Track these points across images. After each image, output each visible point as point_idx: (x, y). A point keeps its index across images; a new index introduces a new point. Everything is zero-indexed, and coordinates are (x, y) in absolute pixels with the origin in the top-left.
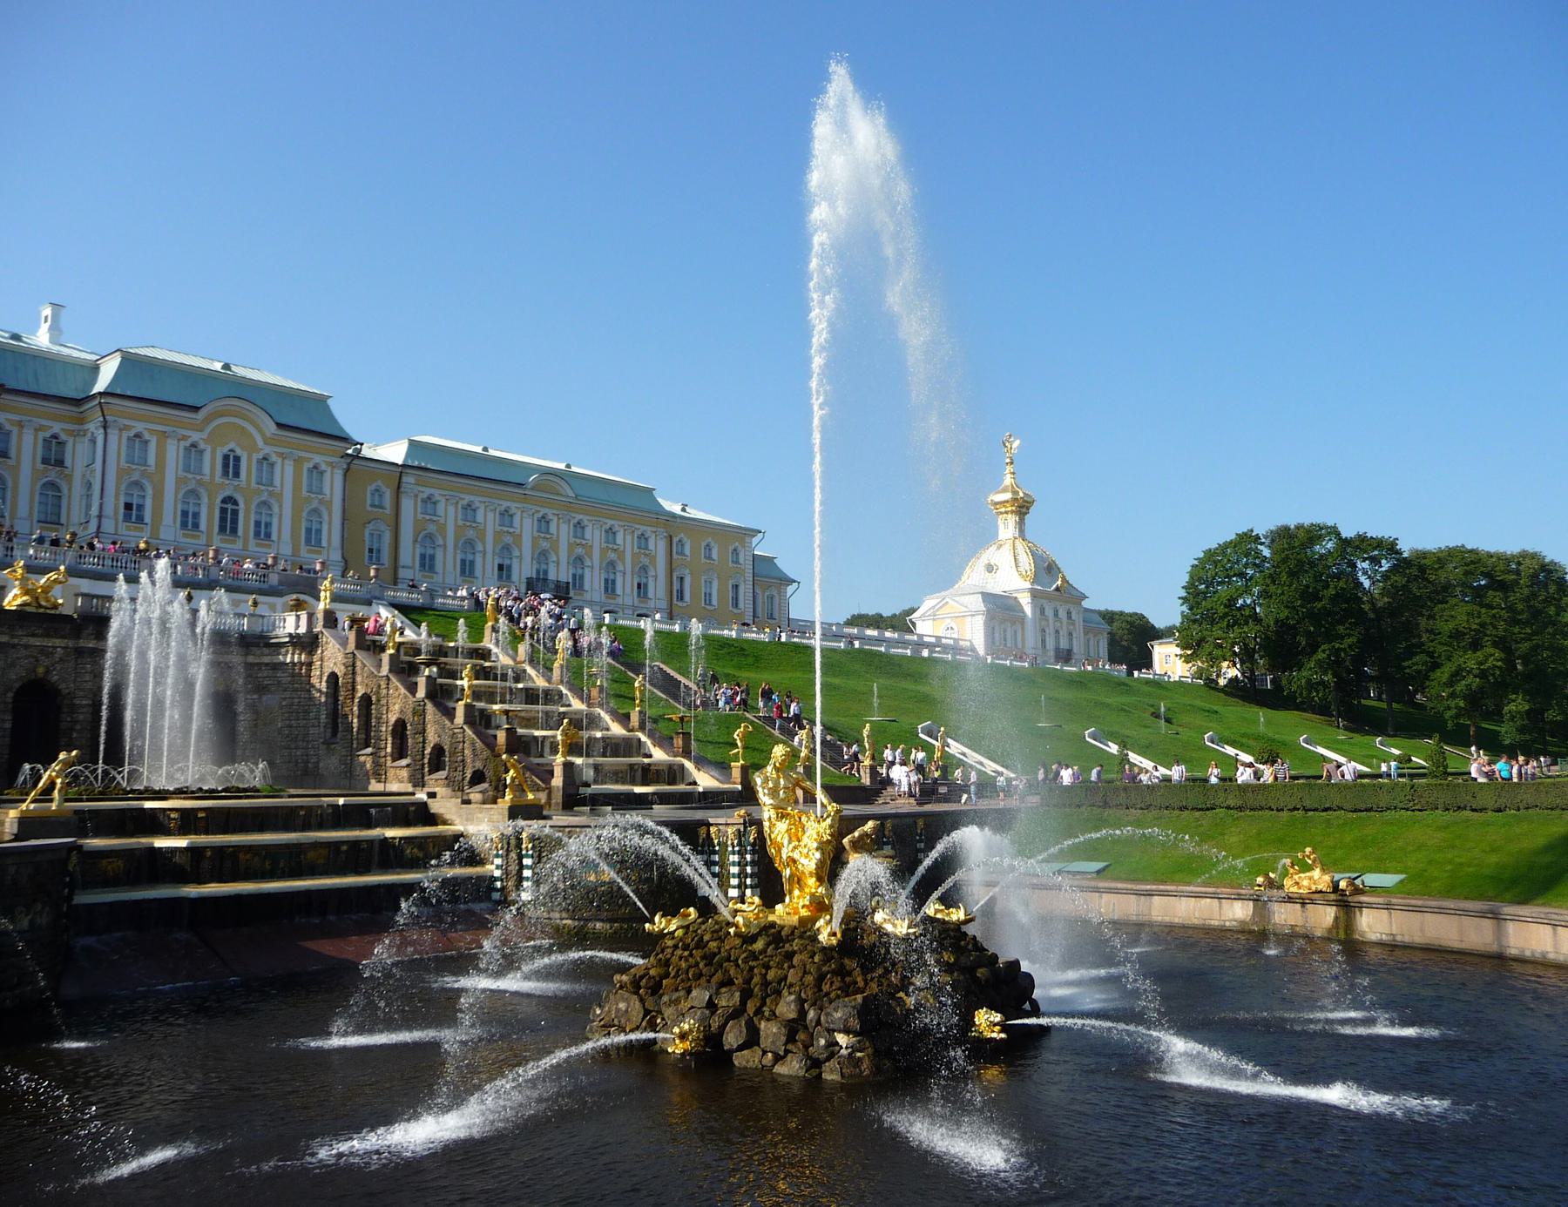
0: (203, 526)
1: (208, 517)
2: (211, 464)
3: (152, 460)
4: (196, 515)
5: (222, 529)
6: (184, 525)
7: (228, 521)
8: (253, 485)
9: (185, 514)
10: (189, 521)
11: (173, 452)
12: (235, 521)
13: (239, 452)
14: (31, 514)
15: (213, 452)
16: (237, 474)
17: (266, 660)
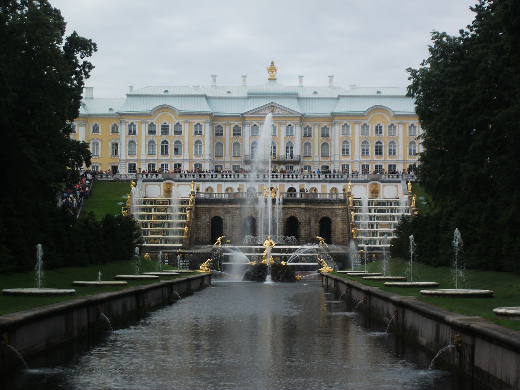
0: (370, 154)
1: (372, 150)
2: (372, 130)
3: (350, 133)
4: (367, 150)
5: (377, 153)
6: (363, 153)
7: (379, 151)
8: (387, 135)
9: (363, 150)
10: (365, 152)
11: (358, 129)
12: (381, 150)
13: (381, 125)
14: (319, 154)
15: (372, 126)
16: (381, 133)
17: (337, 207)
